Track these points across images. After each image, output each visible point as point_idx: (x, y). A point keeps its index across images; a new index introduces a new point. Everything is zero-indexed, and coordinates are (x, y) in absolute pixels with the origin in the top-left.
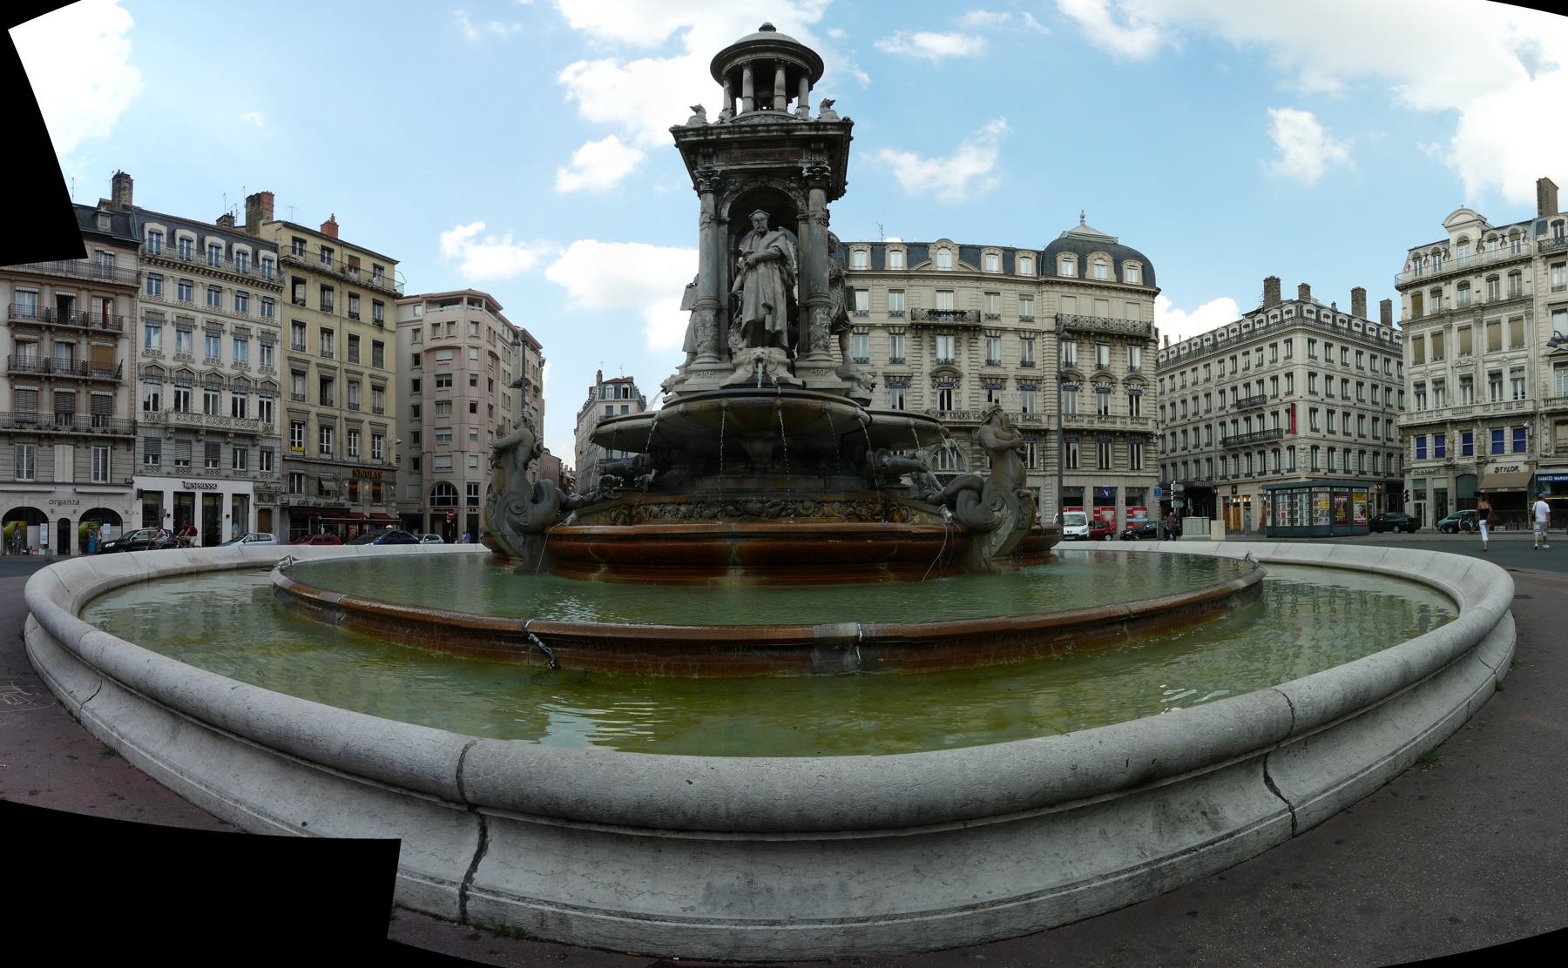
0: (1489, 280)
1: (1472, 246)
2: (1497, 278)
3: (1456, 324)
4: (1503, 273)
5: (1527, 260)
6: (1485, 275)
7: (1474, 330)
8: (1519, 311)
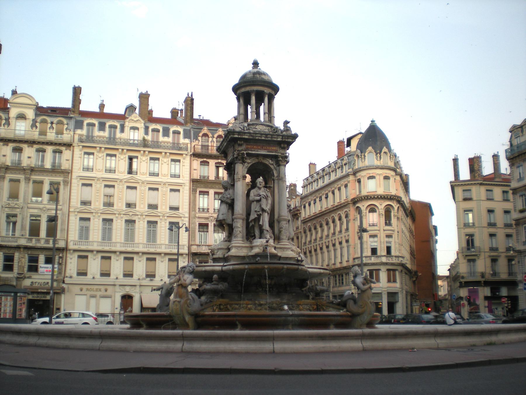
0: (38, 151)
1: (29, 122)
2: (44, 151)
3: (9, 176)
4: (49, 149)
5: (69, 145)
6: (36, 146)
7: (22, 185)
8: (59, 179)
